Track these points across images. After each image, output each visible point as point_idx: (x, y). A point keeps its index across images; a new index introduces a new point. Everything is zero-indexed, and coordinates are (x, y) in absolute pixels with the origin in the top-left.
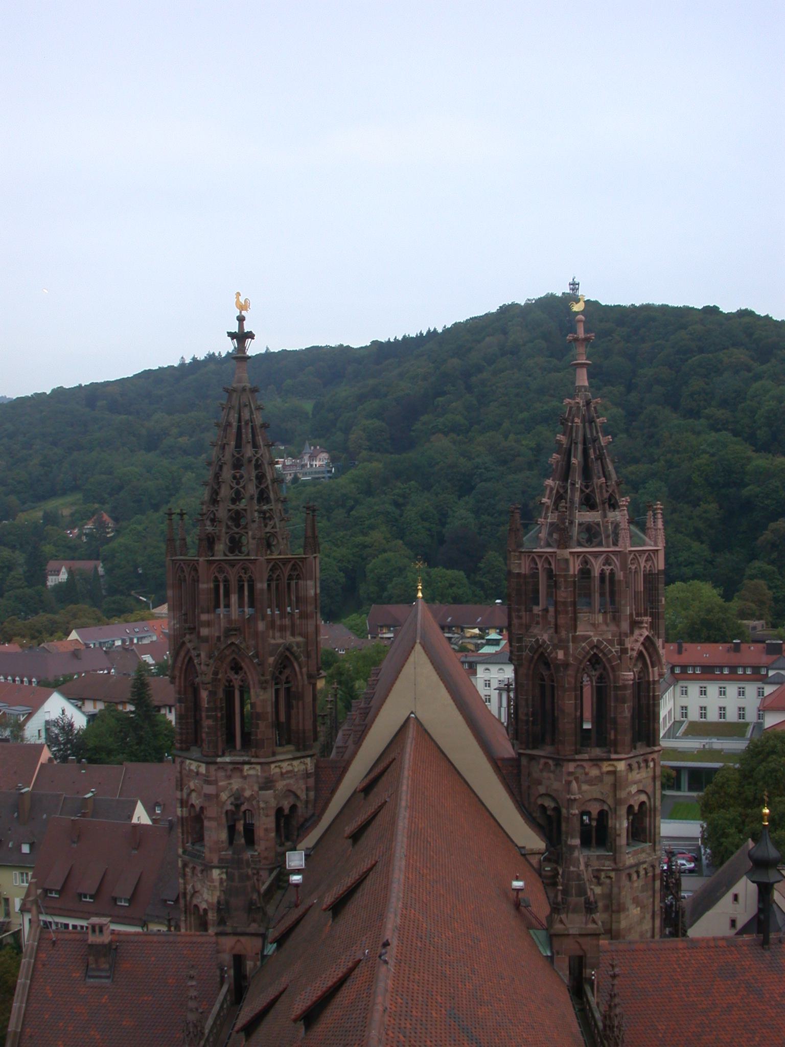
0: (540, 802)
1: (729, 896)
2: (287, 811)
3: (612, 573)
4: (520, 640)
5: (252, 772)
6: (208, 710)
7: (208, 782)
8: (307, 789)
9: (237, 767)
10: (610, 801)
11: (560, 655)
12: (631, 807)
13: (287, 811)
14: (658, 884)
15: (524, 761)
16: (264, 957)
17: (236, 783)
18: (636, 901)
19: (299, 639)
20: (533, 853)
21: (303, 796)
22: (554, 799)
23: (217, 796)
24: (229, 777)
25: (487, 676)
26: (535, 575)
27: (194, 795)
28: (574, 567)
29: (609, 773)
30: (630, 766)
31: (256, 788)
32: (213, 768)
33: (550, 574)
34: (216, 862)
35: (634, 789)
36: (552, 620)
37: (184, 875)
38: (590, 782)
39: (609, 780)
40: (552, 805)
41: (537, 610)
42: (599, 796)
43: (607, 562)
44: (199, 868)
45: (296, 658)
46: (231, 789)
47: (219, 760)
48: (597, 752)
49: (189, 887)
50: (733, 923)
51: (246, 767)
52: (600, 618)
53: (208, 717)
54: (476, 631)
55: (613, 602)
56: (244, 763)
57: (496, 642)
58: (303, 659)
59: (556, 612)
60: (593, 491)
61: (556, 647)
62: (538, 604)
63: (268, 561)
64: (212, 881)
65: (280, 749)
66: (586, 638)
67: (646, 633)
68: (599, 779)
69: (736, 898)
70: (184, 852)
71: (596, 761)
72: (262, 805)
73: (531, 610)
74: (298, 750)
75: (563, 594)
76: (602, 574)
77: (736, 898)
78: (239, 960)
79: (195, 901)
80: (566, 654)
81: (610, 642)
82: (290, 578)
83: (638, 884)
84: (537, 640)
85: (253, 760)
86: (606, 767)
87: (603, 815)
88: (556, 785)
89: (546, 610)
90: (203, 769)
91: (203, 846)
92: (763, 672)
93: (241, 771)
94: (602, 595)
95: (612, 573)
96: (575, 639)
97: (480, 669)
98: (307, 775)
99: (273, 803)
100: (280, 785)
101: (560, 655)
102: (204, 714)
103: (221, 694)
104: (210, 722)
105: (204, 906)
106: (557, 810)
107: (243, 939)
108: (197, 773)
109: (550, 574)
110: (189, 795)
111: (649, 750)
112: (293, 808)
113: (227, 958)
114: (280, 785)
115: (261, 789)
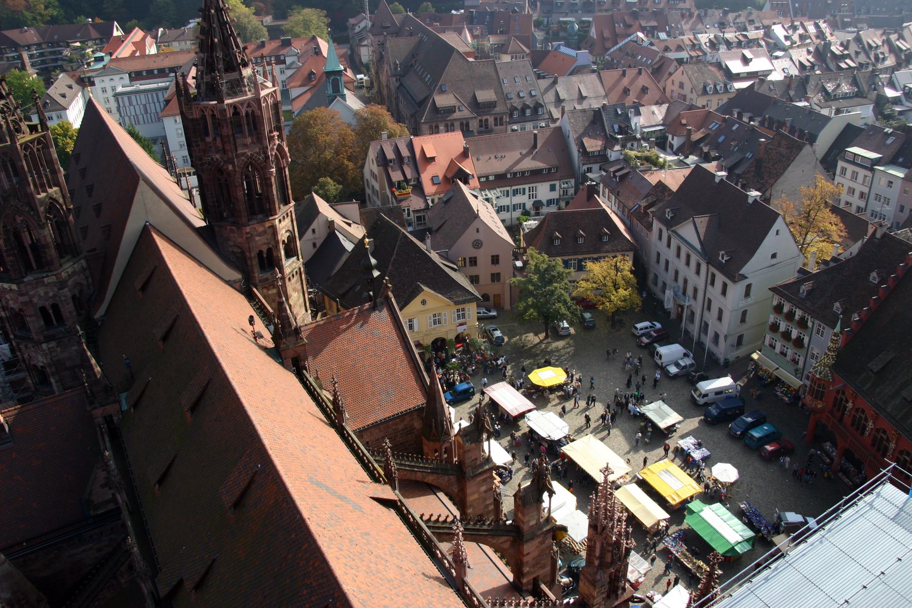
0: (230, 249)
1: (310, 231)
2: (78, 295)
3: (253, 112)
4: (201, 159)
5: (50, 281)
6: (6, 251)
7: (22, 295)
8: (86, 278)
9: (39, 282)
10: (273, 243)
11: (230, 167)
12: (284, 241)
13: (78, 295)
14: (303, 276)
15: (216, 229)
16: (122, 412)
17: (41, 291)
18: (295, 290)
19: (55, 189)
20: (235, 282)
21: (85, 283)
22: (239, 248)
23: (31, 301)
24: (37, 287)
25: (103, 85)
26: (204, 117)
27: (11, 302)
28: (229, 113)
29: (269, 227)
30: (280, 221)
31: (56, 289)
32: (22, 286)
33: (213, 116)
34: (42, 339)
35: (283, 231)
36: (221, 146)
37: (20, 350)
38: (259, 235)
39: (270, 231)
40: (239, 251)
41: (209, 139)
42: (266, 241)
43: (249, 106)
44: (30, 345)
45: (57, 202)
46: (39, 295)
47: (25, 280)
48: (260, 216)
49: (26, 356)
50: (314, 245)
51: (45, 279)
52: (249, 140)
53: (8, 256)
54: (78, 44)
55: (255, 128)
56: (43, 277)
57: (100, 59)
58: (61, 201)
59: (222, 140)
60: (231, 59)
61: (226, 162)
62: (208, 135)
63: (21, 145)
64: (44, 351)
65: (63, 261)
66: (244, 154)
67: (277, 142)
68: (265, 232)
69: (314, 231)
70: (15, 336)
71: (262, 222)
72: (63, 298)
73: (204, 140)
74: (74, 257)
75: (227, 131)
76: (247, 113)
77: (314, 231)
78: (108, 420)
79: (32, 363)
80: (234, 166)
81: (259, 154)
82: (38, 150)
83: (293, 281)
84: (212, 159)
85: (49, 274)
86: (268, 224)
87: (269, 250)
88: (239, 240)
89: (215, 139)
90: (14, 287)
91: (29, 330)
92: (282, 58)
93: (43, 282)
94: (248, 124)
95: (253, 112)
96: (238, 156)
97: (97, 80)
98: (83, 270)
99: (69, 294)
100: (70, 283)
101: (230, 167)
102: (4, 254)
103: (12, 239)
104: (11, 258)
105: (41, 364)
106: (243, 252)
107: (107, 407)
108: (11, 290)
109: (213, 116)
110: (7, 303)
111: (287, 207)
112: (81, 291)
113: (100, 420)
114: (70, 283)
115: (59, 289)
